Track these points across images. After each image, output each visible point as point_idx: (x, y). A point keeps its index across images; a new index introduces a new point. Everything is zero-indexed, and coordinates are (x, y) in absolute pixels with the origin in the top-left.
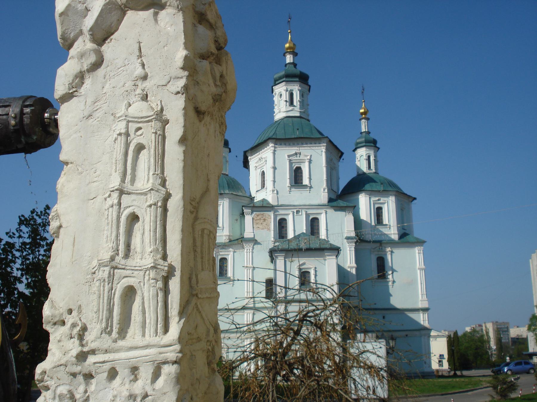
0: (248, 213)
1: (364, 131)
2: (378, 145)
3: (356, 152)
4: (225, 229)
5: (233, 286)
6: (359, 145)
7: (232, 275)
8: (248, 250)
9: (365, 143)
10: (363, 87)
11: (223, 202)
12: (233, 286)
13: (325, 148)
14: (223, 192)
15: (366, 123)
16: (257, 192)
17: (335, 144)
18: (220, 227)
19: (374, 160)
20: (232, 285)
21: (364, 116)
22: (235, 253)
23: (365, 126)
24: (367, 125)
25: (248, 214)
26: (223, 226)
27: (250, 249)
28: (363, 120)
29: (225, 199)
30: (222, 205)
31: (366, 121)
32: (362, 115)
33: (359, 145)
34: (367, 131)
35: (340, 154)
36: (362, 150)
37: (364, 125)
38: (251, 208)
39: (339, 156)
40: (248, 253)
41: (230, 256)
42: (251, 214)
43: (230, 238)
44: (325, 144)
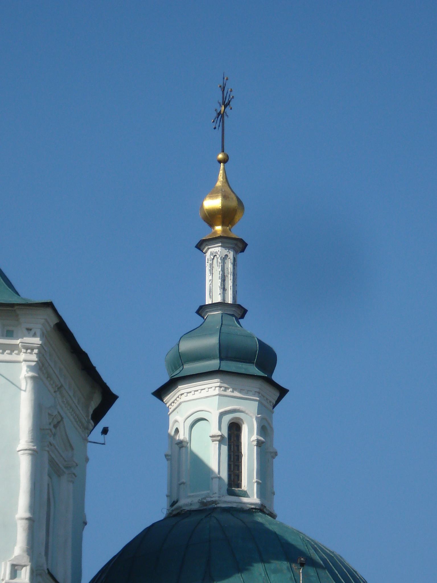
1: (218, 299)
2: (276, 377)
3: (169, 398)
6: (190, 368)
9: (221, 359)
10: (223, 89)
13: (34, 357)
15: (229, 266)
17: (84, 345)
19: (259, 444)
21: (219, 228)
23: (223, 279)
24: (234, 274)
28: (216, 249)
31: (231, 254)
32: (212, 225)
33: (190, 368)
34: (230, 300)
35: (95, 402)
36: (204, 394)
37: (217, 270)
39: (91, 411)
44: (37, 341)
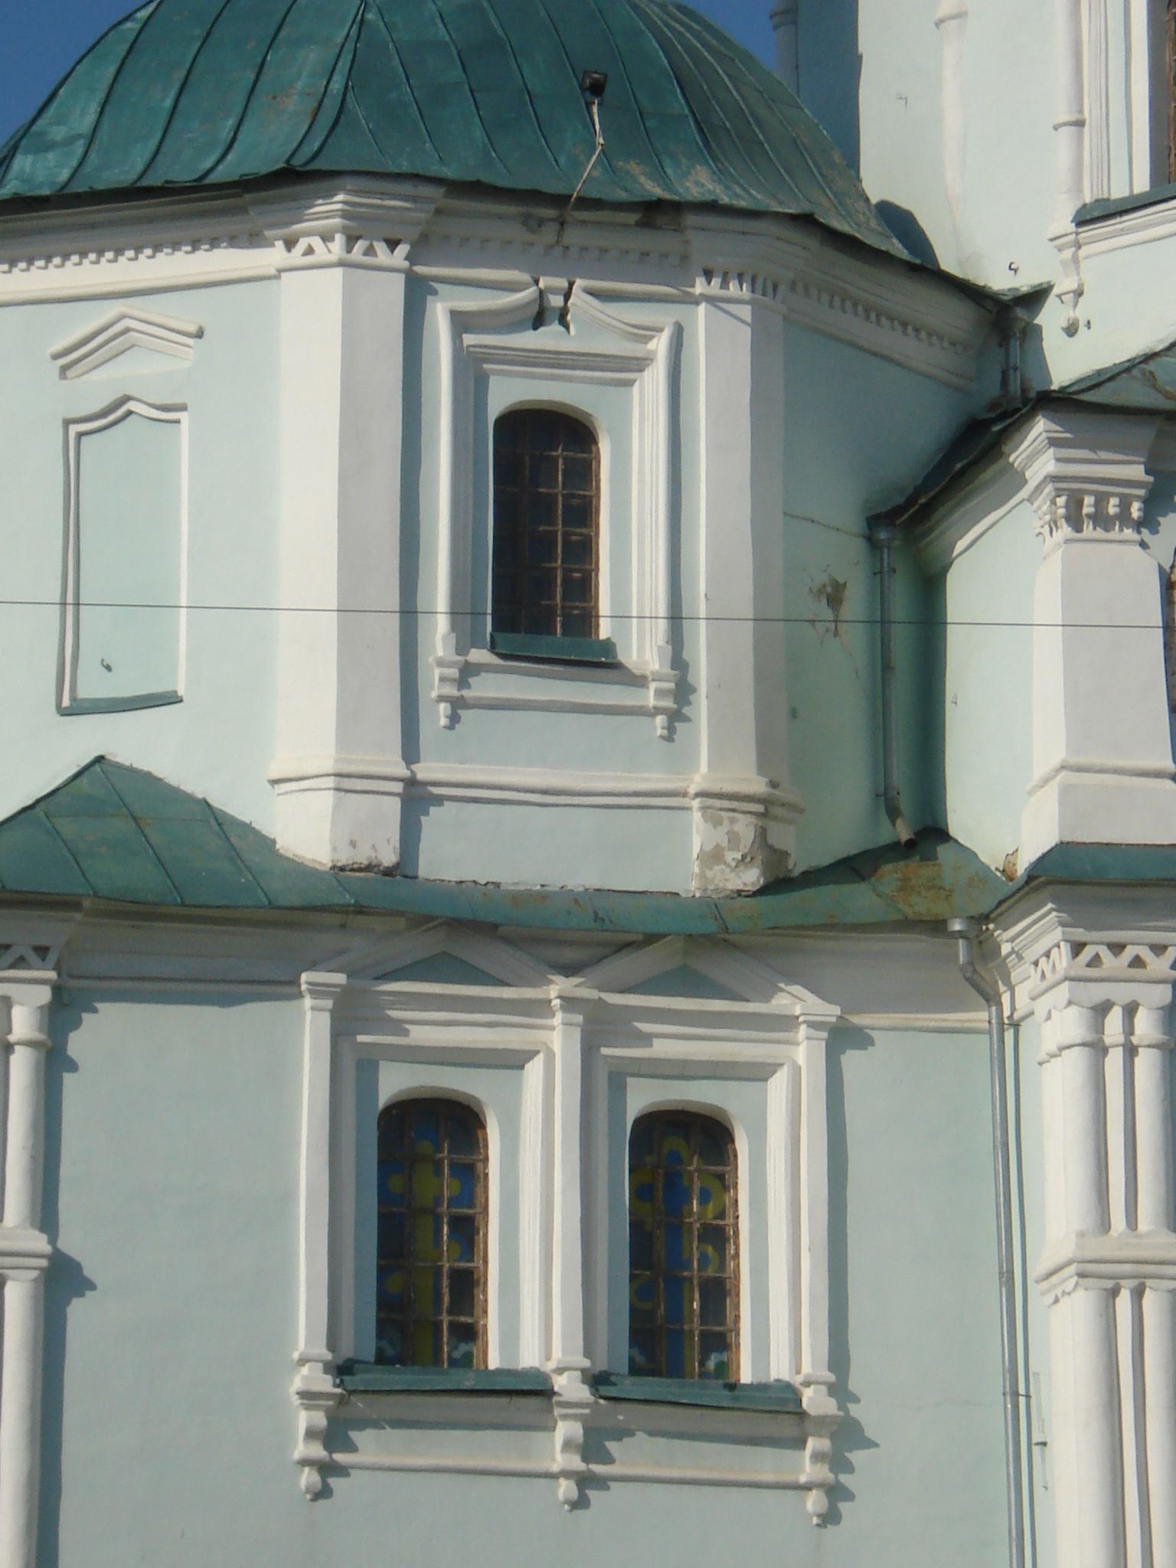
0: (1101, 500)
4: (701, 707)
5: (830, 1518)
7: (813, 1362)
8: (1114, 1021)
11: (679, 333)
12: (830, 1518)
14: (656, 191)
16: (1086, 218)
18: (639, 681)
20: (814, 1502)
22: (852, 1060)
25: (1100, 519)
26: (679, 663)
27: (1130, 1010)
29: (700, 287)
30: (653, 383)
38: (1145, 434)
40: (1114, 1062)
41: (778, 1085)
42: (1148, 522)
43: (783, 837)
